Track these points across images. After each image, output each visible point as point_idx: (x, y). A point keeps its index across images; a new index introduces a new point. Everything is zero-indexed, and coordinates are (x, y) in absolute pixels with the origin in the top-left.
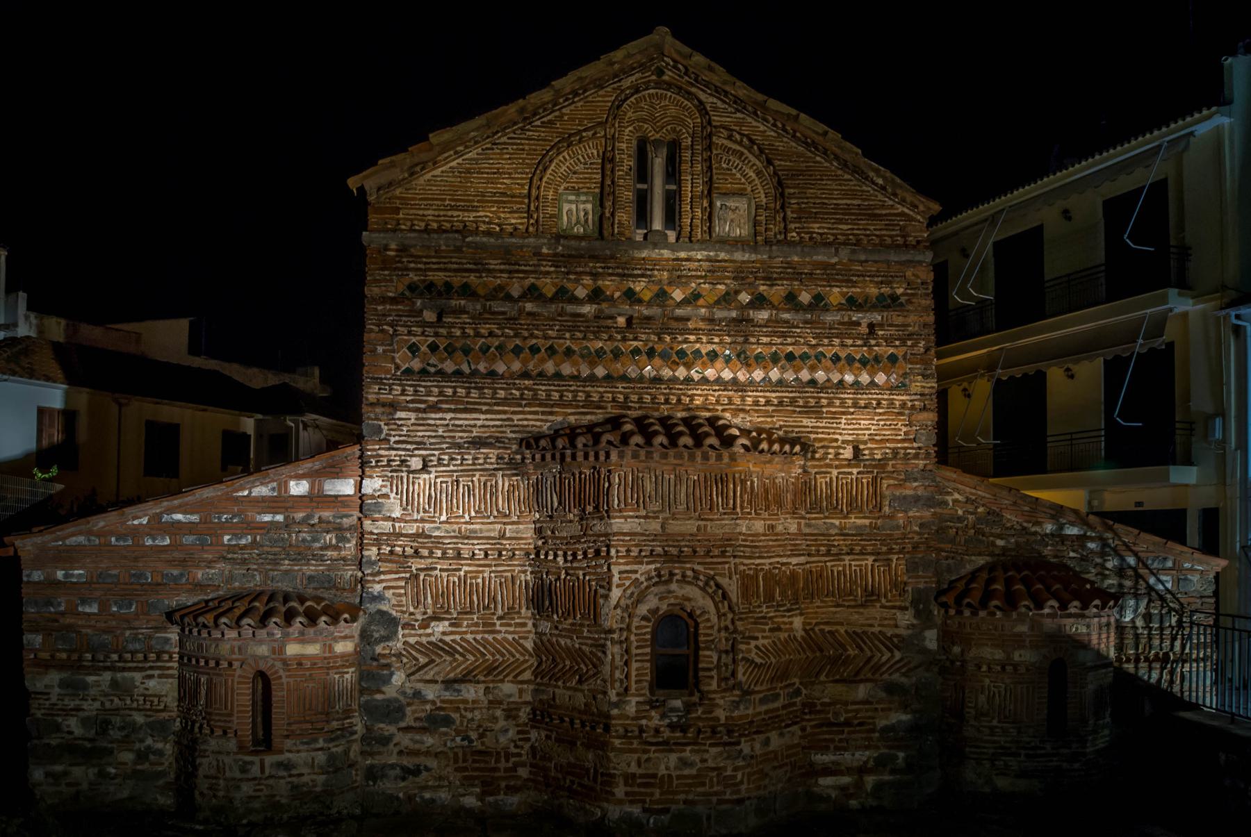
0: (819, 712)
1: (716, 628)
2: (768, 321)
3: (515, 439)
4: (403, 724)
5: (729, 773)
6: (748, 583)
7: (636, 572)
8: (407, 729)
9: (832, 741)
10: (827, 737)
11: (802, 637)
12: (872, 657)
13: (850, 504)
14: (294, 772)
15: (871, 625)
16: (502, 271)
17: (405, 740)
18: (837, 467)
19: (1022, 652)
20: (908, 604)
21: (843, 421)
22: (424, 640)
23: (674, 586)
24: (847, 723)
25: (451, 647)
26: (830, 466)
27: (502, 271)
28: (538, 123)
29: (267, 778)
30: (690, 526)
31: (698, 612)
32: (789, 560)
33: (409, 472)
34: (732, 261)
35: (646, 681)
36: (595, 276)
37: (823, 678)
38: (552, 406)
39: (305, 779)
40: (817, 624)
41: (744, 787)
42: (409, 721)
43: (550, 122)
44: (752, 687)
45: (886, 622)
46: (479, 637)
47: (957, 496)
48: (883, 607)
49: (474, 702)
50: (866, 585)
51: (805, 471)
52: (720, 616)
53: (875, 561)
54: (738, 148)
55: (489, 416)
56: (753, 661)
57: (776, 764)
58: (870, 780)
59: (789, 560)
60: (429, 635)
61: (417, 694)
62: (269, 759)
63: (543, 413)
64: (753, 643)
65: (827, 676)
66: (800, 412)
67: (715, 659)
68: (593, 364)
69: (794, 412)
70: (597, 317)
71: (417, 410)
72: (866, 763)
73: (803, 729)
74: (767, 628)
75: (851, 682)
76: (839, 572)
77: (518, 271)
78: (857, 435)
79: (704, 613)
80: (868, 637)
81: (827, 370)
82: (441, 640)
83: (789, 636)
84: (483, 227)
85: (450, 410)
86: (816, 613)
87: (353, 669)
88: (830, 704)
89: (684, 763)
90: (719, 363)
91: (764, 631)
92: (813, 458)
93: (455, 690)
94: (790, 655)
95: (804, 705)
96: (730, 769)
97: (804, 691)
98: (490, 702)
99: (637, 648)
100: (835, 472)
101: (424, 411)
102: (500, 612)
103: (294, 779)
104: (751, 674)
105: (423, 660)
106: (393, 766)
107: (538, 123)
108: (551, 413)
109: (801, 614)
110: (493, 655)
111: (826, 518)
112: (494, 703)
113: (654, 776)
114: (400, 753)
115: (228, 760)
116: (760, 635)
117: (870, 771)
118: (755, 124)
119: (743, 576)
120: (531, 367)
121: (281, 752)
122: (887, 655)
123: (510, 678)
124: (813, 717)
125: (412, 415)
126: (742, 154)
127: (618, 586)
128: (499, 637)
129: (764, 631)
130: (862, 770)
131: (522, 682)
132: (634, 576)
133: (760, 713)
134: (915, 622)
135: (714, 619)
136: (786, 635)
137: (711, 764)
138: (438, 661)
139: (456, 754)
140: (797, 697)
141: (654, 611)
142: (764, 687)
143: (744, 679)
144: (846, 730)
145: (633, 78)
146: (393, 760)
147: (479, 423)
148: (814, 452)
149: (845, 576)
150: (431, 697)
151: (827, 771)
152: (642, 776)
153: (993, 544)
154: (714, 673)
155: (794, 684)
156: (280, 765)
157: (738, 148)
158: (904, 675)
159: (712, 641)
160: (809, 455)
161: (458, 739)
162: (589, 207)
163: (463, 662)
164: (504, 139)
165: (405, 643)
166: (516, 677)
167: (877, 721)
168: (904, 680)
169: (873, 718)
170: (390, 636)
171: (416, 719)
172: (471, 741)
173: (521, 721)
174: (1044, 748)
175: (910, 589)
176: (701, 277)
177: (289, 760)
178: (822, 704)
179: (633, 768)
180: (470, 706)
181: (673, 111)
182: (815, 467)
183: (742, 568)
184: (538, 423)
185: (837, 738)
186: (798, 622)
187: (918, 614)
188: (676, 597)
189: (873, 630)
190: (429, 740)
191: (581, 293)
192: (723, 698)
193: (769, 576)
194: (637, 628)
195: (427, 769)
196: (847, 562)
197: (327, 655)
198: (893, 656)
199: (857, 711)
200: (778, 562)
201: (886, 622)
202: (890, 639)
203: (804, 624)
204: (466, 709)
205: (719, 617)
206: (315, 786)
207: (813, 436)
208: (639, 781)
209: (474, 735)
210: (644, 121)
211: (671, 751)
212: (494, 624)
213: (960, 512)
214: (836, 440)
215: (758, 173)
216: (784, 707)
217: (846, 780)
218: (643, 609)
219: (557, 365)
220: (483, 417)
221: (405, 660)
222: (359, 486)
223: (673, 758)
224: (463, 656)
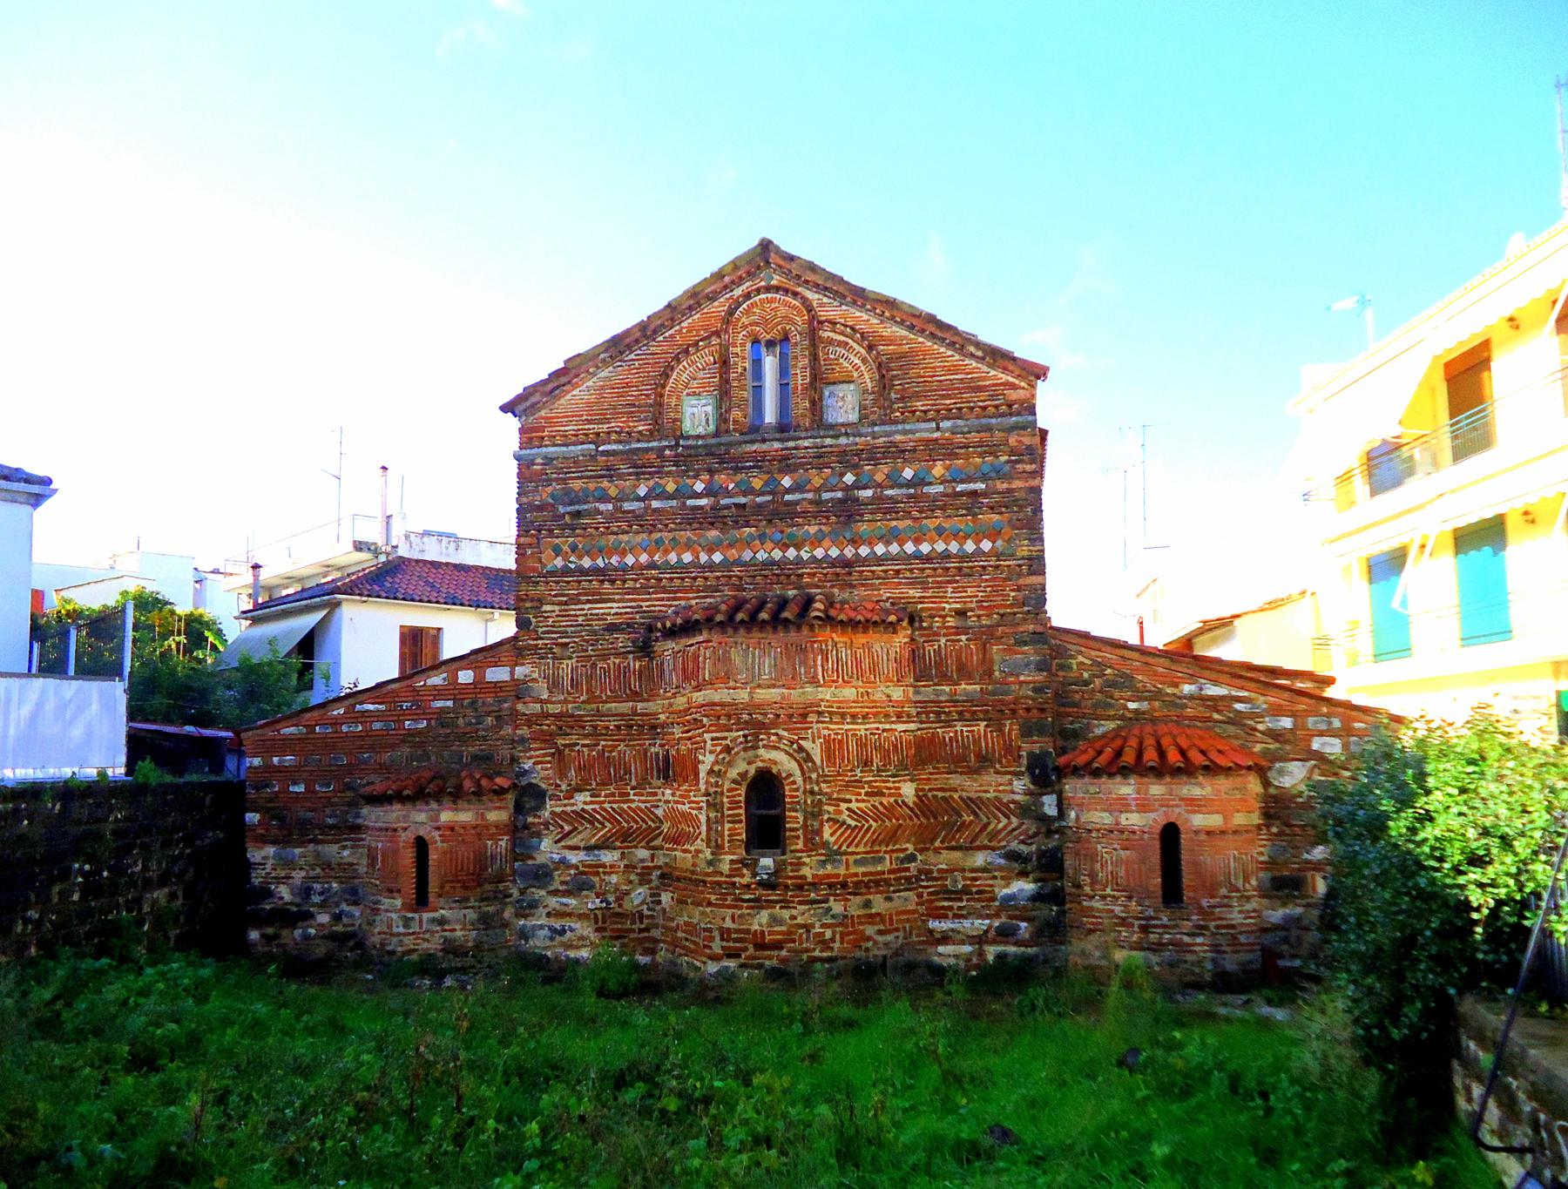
0: (936, 879)
1: (801, 790)
2: (873, 497)
3: (643, 624)
4: (552, 888)
5: (818, 930)
6: (832, 749)
7: (725, 738)
8: (555, 893)
9: (951, 908)
10: (946, 904)
11: (914, 803)
12: (989, 824)
13: (959, 670)
14: (446, 927)
15: (986, 791)
16: (630, 474)
17: (553, 902)
18: (945, 635)
19: (1128, 815)
20: (1023, 769)
21: (950, 590)
22: (569, 809)
23: (762, 751)
24: (966, 891)
25: (591, 816)
26: (939, 635)
27: (630, 474)
28: (661, 338)
29: (424, 933)
30: (773, 694)
31: (784, 775)
32: (894, 726)
33: (553, 658)
34: (836, 446)
35: (742, 841)
36: (711, 472)
37: (937, 844)
38: (676, 592)
39: (459, 933)
40: (930, 790)
41: (837, 945)
42: (556, 885)
43: (671, 336)
44: (844, 848)
45: (1001, 788)
46: (615, 806)
47: (1081, 659)
48: (997, 772)
49: (611, 867)
50: (980, 749)
51: (912, 640)
52: (806, 779)
53: (986, 726)
54: (842, 338)
55: (621, 605)
56: (844, 823)
57: (882, 927)
58: (991, 952)
59: (894, 726)
60: (573, 805)
61: (563, 861)
62: (426, 916)
63: (668, 599)
64: (844, 806)
65: (942, 842)
66: (905, 584)
67: (801, 820)
68: (711, 551)
69: (900, 583)
70: (712, 508)
71: (560, 604)
72: (986, 932)
73: (920, 896)
74: (863, 791)
75: (967, 849)
76: (951, 738)
77: (644, 473)
78: (965, 602)
79: (790, 775)
80: (983, 803)
81: (932, 541)
82: (583, 810)
83: (896, 801)
84: (614, 437)
85: (589, 602)
86: (929, 779)
87: (506, 838)
88: (946, 871)
89: (774, 920)
90: (826, 543)
91: (860, 794)
92: (922, 628)
93: (595, 855)
94: (897, 820)
95: (920, 871)
96: (818, 924)
97: (919, 857)
98: (626, 866)
99: (729, 809)
100: (943, 640)
101: (566, 603)
102: (634, 783)
103: (447, 934)
104: (842, 834)
105: (567, 828)
106: (541, 927)
107: (661, 338)
108: (675, 599)
109: (912, 780)
110: (628, 822)
111: (935, 685)
112: (630, 868)
113: (748, 932)
114: (549, 915)
115: (394, 916)
116: (853, 798)
117: (994, 942)
118: (858, 314)
119: (827, 740)
120: (656, 558)
121: (435, 910)
122: (1004, 821)
123: (643, 844)
124: (930, 883)
125: (556, 608)
126: (847, 344)
127: (711, 752)
128: (633, 806)
129: (860, 794)
130: (980, 940)
131: (654, 848)
132: (724, 742)
133: (856, 875)
134: (1032, 787)
135: (799, 780)
136: (892, 800)
137: (800, 920)
138: (580, 828)
139: (596, 916)
140: (909, 862)
141: (743, 775)
142: (861, 849)
143: (833, 839)
144: (965, 897)
145: (744, 287)
146: (543, 921)
147: (613, 611)
148: (921, 621)
149: (957, 741)
150: (574, 861)
151: (945, 939)
152: (737, 931)
153: (1126, 708)
154: (800, 833)
155: (907, 849)
156: (433, 920)
157: (842, 338)
158: (1023, 842)
159: (798, 803)
160: (917, 625)
161: (598, 901)
162: (709, 409)
163: (602, 829)
164: (632, 356)
165: (553, 813)
166: (648, 843)
167: (996, 890)
168: (1023, 847)
169: (991, 886)
170: (541, 805)
171: (562, 883)
172: (608, 903)
173: (653, 885)
174: (1157, 919)
175: (1024, 753)
176: (807, 464)
177: (442, 916)
178: (940, 871)
179: (728, 924)
180: (608, 870)
181: (783, 311)
182: (922, 636)
183: (826, 732)
184: (664, 609)
185: (956, 904)
186: (908, 790)
187: (1035, 781)
188: (763, 761)
189: (988, 795)
190: (573, 902)
191: (699, 487)
192: (809, 856)
193: (862, 744)
194: (729, 791)
195: (572, 930)
196: (958, 728)
197: (479, 822)
198: (1010, 823)
199: (975, 879)
200: (878, 729)
201: (1001, 788)
202: (1006, 805)
203: (917, 790)
204: (604, 873)
205: (804, 781)
206: (467, 941)
207: (920, 606)
208: (734, 936)
209: (611, 898)
210: (757, 324)
211: (763, 908)
212: (629, 794)
213: (1086, 675)
214: (944, 609)
215: (864, 361)
216: (891, 872)
217: (967, 949)
218: (733, 773)
219: (679, 555)
220: (615, 605)
221: (552, 828)
222: (512, 673)
223: (764, 916)
224: (602, 824)
